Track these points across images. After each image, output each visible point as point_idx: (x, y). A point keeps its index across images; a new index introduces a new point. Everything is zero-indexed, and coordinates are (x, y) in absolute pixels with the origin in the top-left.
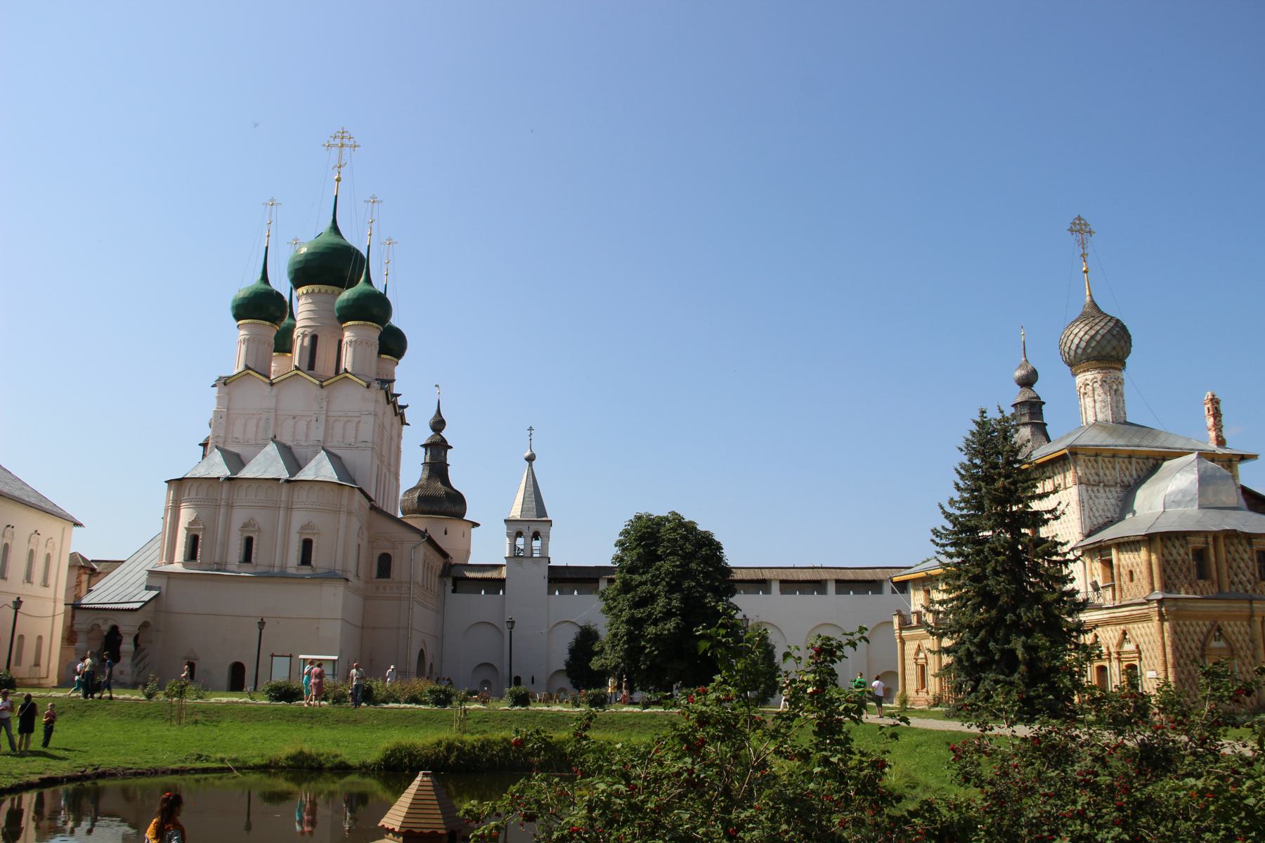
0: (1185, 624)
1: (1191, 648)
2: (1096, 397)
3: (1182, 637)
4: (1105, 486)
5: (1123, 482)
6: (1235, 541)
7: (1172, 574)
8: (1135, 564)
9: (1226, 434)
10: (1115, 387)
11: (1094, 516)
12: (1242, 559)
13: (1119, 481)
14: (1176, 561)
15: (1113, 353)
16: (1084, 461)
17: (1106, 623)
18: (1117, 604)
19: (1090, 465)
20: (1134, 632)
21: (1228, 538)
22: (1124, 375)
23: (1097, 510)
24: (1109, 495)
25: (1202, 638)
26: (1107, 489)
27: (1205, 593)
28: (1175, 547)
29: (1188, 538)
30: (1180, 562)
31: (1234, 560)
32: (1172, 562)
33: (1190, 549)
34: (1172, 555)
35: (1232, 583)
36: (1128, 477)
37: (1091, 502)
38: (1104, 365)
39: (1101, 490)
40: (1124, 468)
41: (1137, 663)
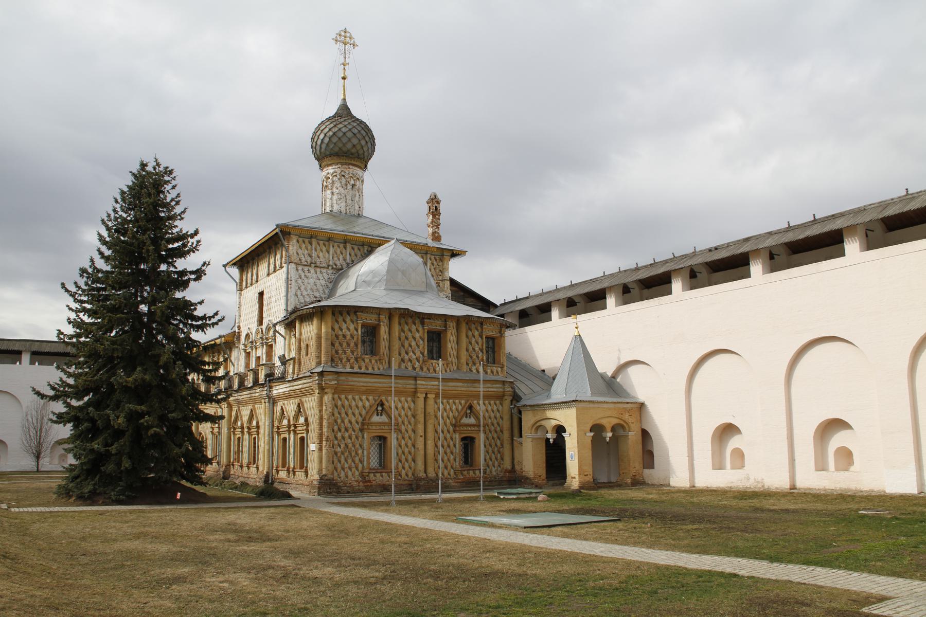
0: (347, 398)
1: (350, 422)
2: (334, 190)
3: (343, 411)
4: (315, 266)
5: (336, 265)
6: (410, 320)
7: (340, 348)
9: (442, 232)
10: (352, 182)
12: (414, 338)
13: (331, 263)
14: (344, 336)
15: (354, 151)
16: (298, 241)
17: (288, 396)
18: (295, 378)
19: (304, 246)
20: (305, 406)
21: (404, 318)
22: (367, 176)
25: (364, 412)
26: (318, 270)
27: (370, 368)
29: (358, 313)
30: (348, 337)
31: (407, 338)
32: (341, 337)
33: (360, 325)
34: (341, 330)
35: (403, 360)
37: (300, 281)
38: (344, 161)
39: (312, 271)
41: (305, 435)
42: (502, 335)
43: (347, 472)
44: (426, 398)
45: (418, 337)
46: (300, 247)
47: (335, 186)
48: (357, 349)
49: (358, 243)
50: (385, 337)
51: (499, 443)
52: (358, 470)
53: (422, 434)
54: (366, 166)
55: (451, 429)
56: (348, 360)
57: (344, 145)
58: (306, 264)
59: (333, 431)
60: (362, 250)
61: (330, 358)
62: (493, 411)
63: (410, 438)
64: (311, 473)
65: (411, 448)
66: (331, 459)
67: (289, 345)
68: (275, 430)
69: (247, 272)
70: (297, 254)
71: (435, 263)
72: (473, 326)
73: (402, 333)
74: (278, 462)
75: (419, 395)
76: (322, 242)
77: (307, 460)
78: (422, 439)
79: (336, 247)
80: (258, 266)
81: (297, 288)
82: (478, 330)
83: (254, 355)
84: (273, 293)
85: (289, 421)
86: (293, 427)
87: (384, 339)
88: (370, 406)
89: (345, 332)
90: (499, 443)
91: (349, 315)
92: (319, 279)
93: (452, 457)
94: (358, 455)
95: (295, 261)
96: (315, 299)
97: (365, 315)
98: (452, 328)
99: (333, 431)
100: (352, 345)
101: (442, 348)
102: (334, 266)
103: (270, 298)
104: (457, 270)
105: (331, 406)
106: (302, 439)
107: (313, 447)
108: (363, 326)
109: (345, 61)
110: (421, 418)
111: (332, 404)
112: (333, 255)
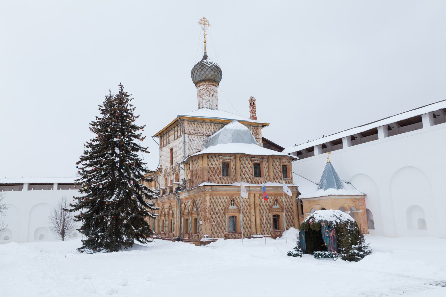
0: (216, 198)
1: (219, 210)
3: (215, 204)
4: (197, 135)
5: (207, 134)
6: (245, 159)
7: (212, 174)
8: (197, 170)
9: (257, 115)
10: (212, 93)
11: (191, 149)
12: (247, 167)
13: (205, 133)
14: (214, 168)
16: (188, 123)
19: (191, 125)
21: (242, 157)
22: (219, 89)
23: (193, 146)
24: (200, 140)
26: (199, 137)
28: (214, 161)
29: (220, 157)
30: (216, 168)
31: (244, 168)
32: (212, 168)
33: (221, 162)
34: (212, 165)
35: (242, 178)
36: (210, 132)
37: (190, 142)
38: (208, 83)
39: (196, 137)
40: (208, 127)
42: (290, 164)
43: (218, 234)
44: (254, 197)
45: (249, 166)
46: (190, 126)
47: (204, 96)
48: (221, 174)
49: (217, 123)
50: (233, 167)
51: (292, 217)
52: (223, 233)
53: (253, 214)
54: (218, 85)
55: (268, 211)
56: (216, 179)
57: (207, 75)
58: (193, 134)
59: (211, 214)
60: (219, 126)
61: (207, 179)
62: (288, 201)
63: (248, 216)
64: (201, 236)
65: (248, 221)
66: (210, 228)
67: (187, 173)
68: (182, 214)
69: (164, 139)
70: (188, 129)
71: (254, 130)
72: (276, 160)
73: (241, 165)
74: (183, 231)
75: (251, 195)
76: (200, 123)
77: (199, 229)
78: (254, 217)
79: (206, 125)
80: (169, 136)
81: (189, 146)
82: (278, 162)
83: (169, 179)
84: (177, 149)
85: (188, 210)
86: (191, 213)
87: (233, 168)
88: (228, 201)
89: (214, 166)
90: (292, 217)
91: (216, 158)
92: (199, 141)
93: (269, 225)
94: (223, 226)
95: (187, 133)
96: (198, 151)
97: (223, 157)
98: (265, 162)
99: (211, 214)
100: (218, 172)
101: (261, 172)
102: (206, 135)
103: (176, 151)
104: (265, 133)
105: (209, 202)
106: (196, 219)
107: (201, 223)
108: (222, 163)
109: (205, 33)
110: (253, 206)
111: (210, 201)
112: (205, 129)
